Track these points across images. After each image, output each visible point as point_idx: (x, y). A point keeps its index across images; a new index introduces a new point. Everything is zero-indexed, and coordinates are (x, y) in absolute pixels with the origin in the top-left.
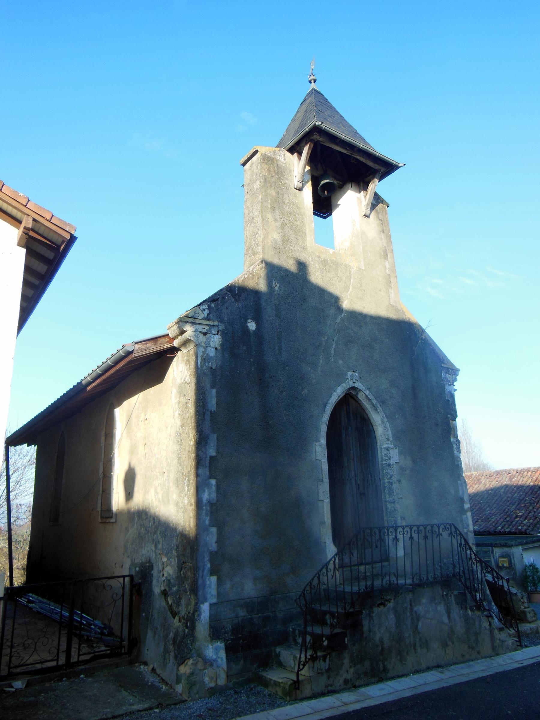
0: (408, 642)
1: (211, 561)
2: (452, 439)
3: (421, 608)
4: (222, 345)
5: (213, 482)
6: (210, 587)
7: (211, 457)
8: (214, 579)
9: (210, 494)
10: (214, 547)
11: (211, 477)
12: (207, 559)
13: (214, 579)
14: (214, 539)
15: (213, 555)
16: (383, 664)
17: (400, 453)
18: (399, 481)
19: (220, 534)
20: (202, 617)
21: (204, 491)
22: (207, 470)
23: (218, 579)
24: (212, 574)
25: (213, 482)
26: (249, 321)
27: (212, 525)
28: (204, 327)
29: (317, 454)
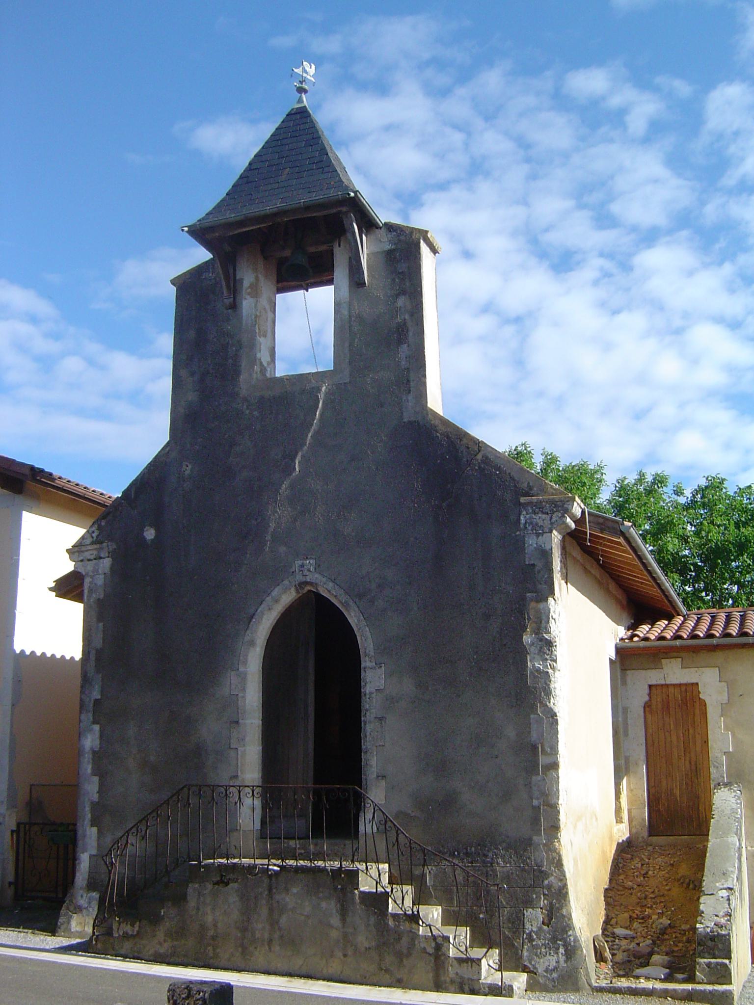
0: (258, 935)
1: (93, 810)
2: (527, 639)
3: (287, 899)
4: (111, 569)
5: (97, 728)
6: (91, 838)
7: (96, 700)
8: (95, 830)
9: (93, 740)
10: (95, 797)
11: (94, 723)
12: (88, 809)
13: (95, 830)
14: (96, 789)
15: (95, 806)
16: (214, 950)
17: (389, 675)
18: (381, 719)
19: (101, 784)
20: (82, 866)
21: (86, 738)
22: (90, 715)
23: (99, 831)
24: (92, 825)
25: (97, 728)
26: (147, 528)
27: (94, 774)
28: (91, 552)
29: (233, 687)
